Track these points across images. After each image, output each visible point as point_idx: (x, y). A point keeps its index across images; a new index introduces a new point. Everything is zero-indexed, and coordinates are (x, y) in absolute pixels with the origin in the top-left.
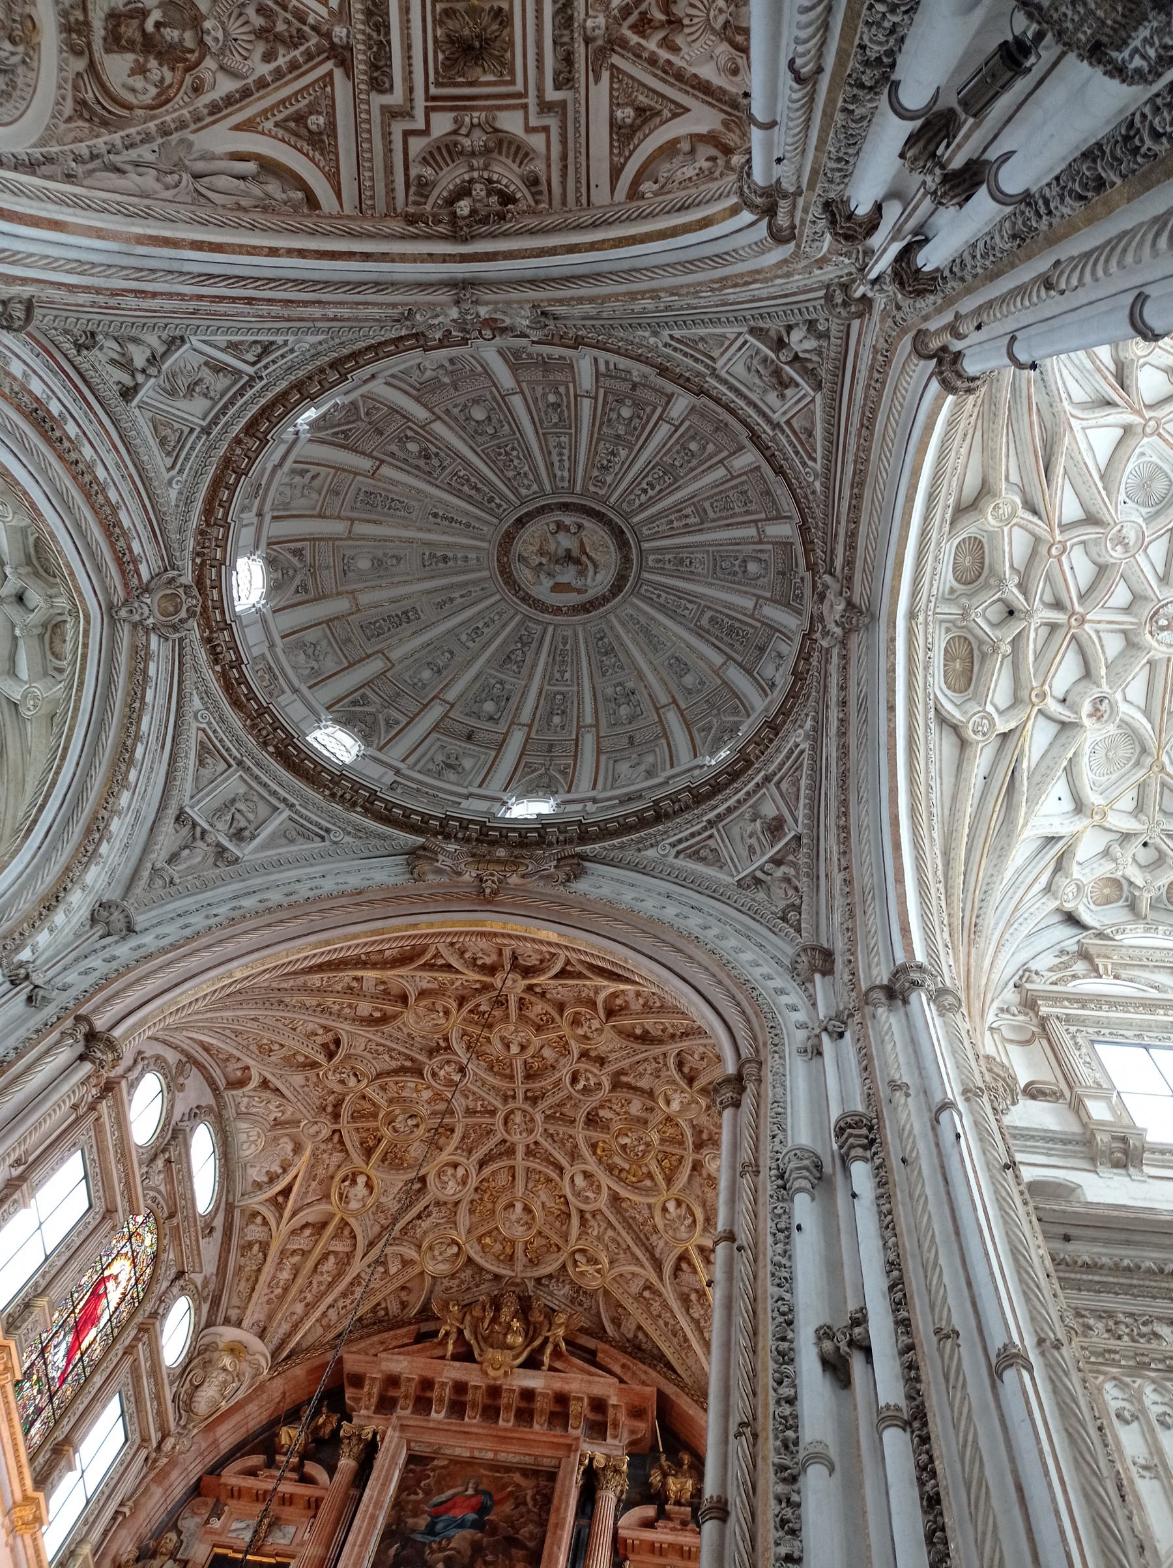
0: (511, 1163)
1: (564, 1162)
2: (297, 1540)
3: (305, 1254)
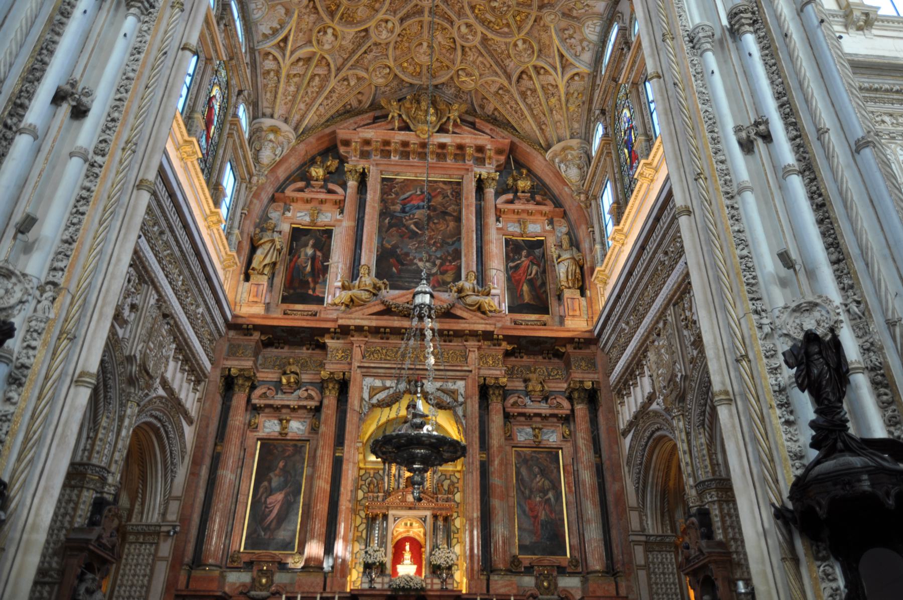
0: (421, 19)
1: (454, 18)
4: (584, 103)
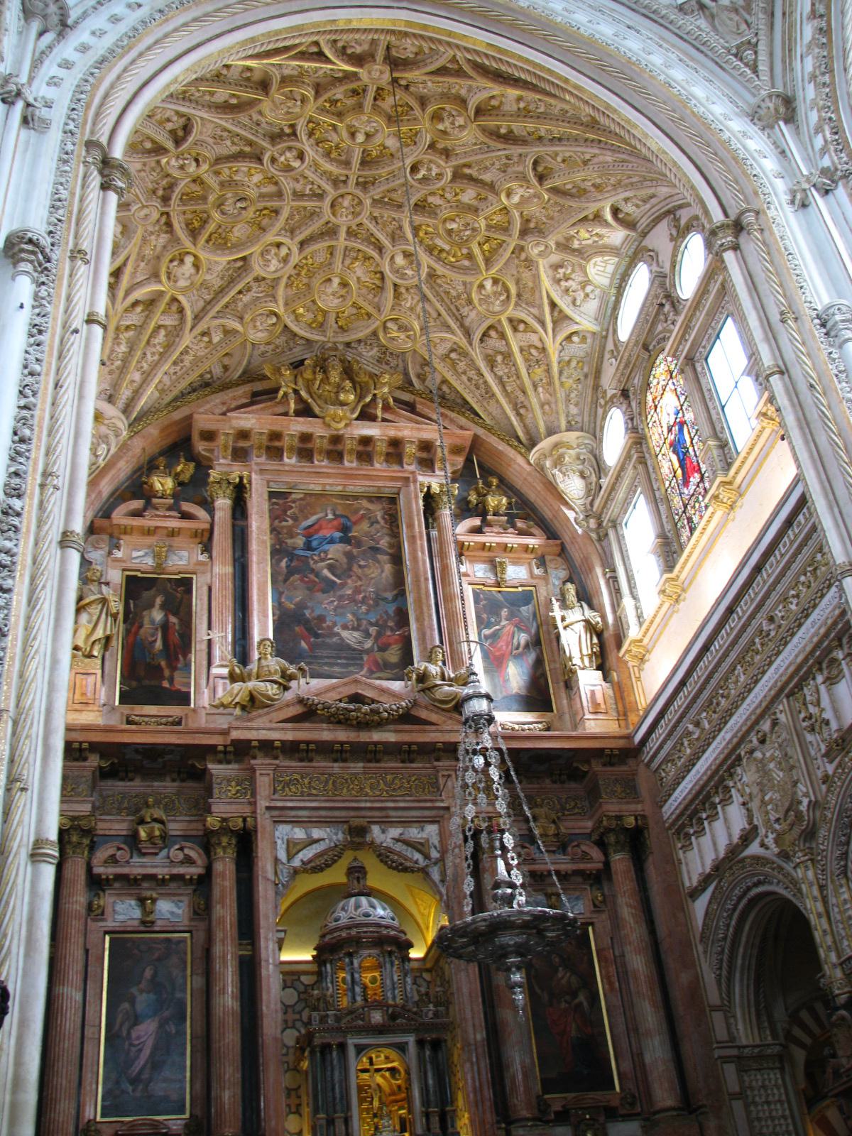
1: (386, 242)
2: (194, 560)
3: (140, 328)
4: (586, 376)
